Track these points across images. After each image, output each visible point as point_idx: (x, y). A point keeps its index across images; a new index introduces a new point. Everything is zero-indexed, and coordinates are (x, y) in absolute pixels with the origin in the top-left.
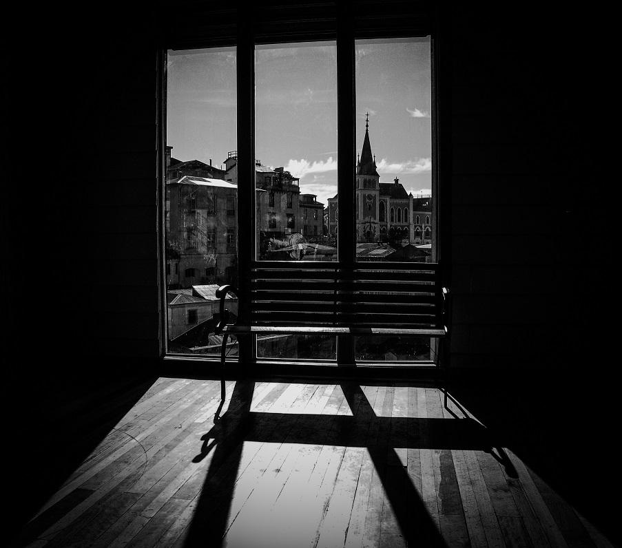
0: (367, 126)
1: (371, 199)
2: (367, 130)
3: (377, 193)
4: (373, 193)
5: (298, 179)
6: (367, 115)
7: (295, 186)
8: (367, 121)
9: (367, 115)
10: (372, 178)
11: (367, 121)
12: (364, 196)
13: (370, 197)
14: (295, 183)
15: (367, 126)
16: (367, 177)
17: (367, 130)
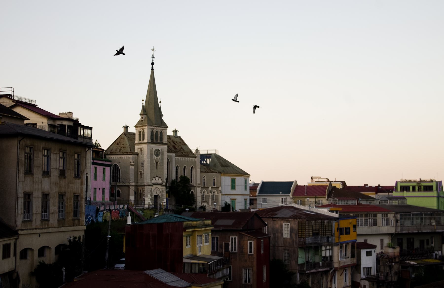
0: (153, 64)
1: (157, 155)
2: (152, 69)
3: (165, 148)
4: (160, 147)
5: (91, 129)
6: (153, 50)
7: (83, 137)
8: (153, 57)
9: (153, 50)
10: (159, 129)
11: (153, 57)
12: (151, 151)
13: (157, 153)
14: (87, 132)
15: (153, 64)
16: (155, 129)
17: (152, 69)
